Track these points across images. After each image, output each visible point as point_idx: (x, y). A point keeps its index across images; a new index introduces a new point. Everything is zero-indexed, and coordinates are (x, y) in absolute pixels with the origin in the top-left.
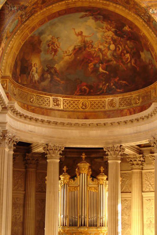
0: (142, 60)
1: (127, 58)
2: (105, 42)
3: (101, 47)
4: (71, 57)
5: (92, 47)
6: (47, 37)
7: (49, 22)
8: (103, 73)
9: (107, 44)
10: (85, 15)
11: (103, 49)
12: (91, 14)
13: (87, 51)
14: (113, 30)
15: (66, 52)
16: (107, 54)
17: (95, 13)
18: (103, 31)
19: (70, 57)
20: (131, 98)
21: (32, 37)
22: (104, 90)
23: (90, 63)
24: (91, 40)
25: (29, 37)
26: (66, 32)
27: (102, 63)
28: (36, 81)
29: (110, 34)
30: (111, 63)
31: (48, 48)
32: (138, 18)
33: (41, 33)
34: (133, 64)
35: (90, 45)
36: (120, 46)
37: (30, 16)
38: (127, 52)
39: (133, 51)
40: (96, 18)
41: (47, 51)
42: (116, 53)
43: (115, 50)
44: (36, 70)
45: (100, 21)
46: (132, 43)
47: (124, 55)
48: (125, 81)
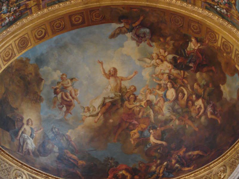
0: (226, 99)
1: (198, 109)
2: (157, 87)
3: (151, 97)
4: (98, 119)
5: (135, 99)
6: (52, 74)
7: (55, 38)
8: (157, 145)
9: (161, 90)
10: (118, 31)
11: (155, 102)
12: (128, 27)
13: (126, 107)
14: (170, 57)
15: (89, 110)
16: (162, 109)
17: (135, 23)
18: (153, 64)
19: (96, 120)
20: (210, 175)
21: (23, 62)
22: (159, 174)
23: (132, 130)
24: (132, 86)
25: (16, 58)
26: (87, 69)
27: (154, 128)
28: (30, 151)
29: (166, 67)
30: (171, 124)
31: (55, 97)
32: (211, 14)
33: (40, 61)
34: (209, 116)
35: (132, 96)
36: (184, 90)
37: (17, 14)
38: (198, 97)
39: (208, 90)
40: (138, 36)
41: (53, 103)
42: (178, 104)
43: (177, 98)
44: (30, 131)
45: (146, 42)
46: (204, 75)
47: (193, 104)
48: (198, 150)
